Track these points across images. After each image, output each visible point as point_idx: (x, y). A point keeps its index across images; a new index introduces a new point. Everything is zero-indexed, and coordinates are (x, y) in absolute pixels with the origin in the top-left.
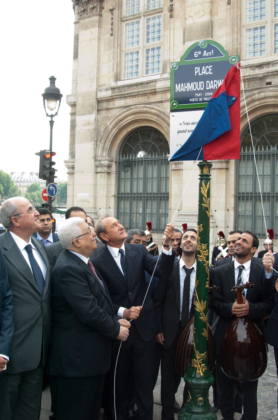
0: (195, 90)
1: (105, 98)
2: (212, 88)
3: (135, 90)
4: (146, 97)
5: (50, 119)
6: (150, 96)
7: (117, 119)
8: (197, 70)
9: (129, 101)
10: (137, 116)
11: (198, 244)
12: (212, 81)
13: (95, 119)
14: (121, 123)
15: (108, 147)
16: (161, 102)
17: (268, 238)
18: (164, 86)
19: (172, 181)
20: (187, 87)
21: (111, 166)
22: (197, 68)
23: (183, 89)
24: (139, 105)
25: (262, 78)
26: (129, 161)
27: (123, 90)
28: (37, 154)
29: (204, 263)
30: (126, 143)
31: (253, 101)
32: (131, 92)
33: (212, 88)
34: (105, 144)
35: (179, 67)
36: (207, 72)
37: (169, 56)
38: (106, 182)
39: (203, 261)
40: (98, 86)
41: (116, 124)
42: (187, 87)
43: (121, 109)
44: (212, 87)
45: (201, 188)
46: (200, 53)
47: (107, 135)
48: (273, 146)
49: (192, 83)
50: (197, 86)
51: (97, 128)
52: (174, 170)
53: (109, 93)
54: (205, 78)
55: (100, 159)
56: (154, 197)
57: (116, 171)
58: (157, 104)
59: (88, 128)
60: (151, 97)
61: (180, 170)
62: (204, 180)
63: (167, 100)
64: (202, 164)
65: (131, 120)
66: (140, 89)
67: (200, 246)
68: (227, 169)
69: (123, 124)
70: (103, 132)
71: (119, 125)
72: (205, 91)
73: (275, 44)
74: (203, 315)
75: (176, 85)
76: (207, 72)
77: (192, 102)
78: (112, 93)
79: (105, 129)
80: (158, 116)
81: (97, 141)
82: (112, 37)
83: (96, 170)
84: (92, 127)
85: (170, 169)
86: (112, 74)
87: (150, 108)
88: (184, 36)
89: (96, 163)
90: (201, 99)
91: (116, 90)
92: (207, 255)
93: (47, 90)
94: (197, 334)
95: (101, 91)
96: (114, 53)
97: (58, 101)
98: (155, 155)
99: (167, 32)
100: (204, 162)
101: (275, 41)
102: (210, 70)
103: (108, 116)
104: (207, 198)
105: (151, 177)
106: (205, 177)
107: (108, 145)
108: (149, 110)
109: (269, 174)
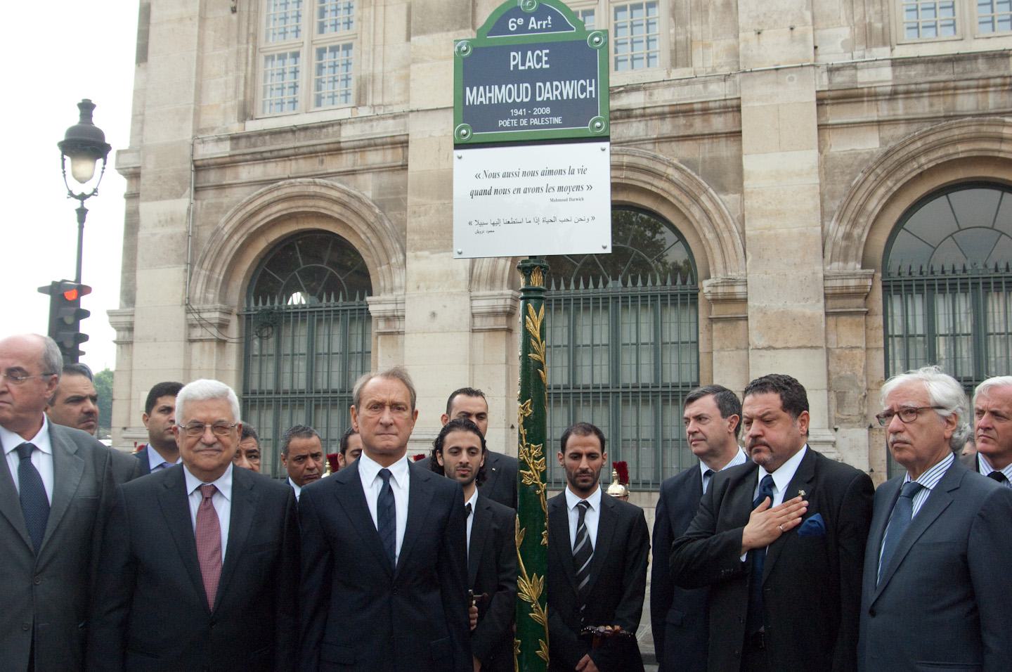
0: (510, 101)
1: (213, 161)
2: (548, 98)
3: (289, 143)
4: (316, 161)
5: (77, 204)
6: (324, 158)
7: (244, 212)
8: (515, 59)
9: (274, 170)
10: (292, 204)
11: (522, 444)
12: (548, 84)
13: (189, 210)
14: (255, 220)
15: (221, 278)
16: (353, 173)
17: (616, 482)
18: (360, 136)
19: (379, 360)
20: (492, 95)
21: (227, 325)
22: (515, 54)
23: (483, 99)
24: (299, 180)
26: (271, 313)
27: (259, 143)
28: (42, 290)
29: (537, 487)
30: (264, 274)
32: (278, 147)
33: (548, 98)
34: (212, 270)
35: (474, 50)
36: (538, 64)
37: (373, 67)
38: (214, 362)
39: (533, 483)
40: (198, 130)
41: (242, 223)
42: (492, 95)
43: (254, 187)
44: (550, 95)
45: (527, 317)
46: (521, 21)
47: (218, 249)
48: (615, 278)
49: (504, 86)
50: (514, 93)
51: (193, 232)
52: (384, 334)
53: (225, 149)
54: (532, 76)
55: (200, 307)
56: (334, 399)
57: (240, 338)
58: (341, 177)
59: (169, 230)
60: (328, 159)
61: (399, 333)
62: (532, 301)
63: (367, 169)
64: (528, 264)
65: (278, 215)
66: (302, 141)
67: (527, 449)
68: (509, 331)
69: (258, 222)
70: (209, 243)
71: (249, 225)
72: (533, 103)
73: (616, 51)
74: (537, 608)
75: (468, 89)
76: (538, 64)
77: (503, 128)
78: (232, 149)
79: (213, 234)
80: (344, 205)
81: (192, 265)
82: (234, 17)
83: (189, 334)
84: (181, 229)
85: (374, 331)
86: (232, 103)
87: (326, 186)
88: (409, 21)
89: (190, 316)
90: (524, 122)
91: (243, 142)
92: (543, 469)
93: (71, 132)
94: (524, 654)
95: (203, 142)
96: (238, 52)
97: (100, 161)
98: (337, 299)
99: (368, 12)
100: (532, 260)
101: (616, 43)
102: (545, 59)
103: (222, 203)
104: (539, 340)
105: (326, 351)
106: (533, 294)
107: (220, 273)
108: (323, 191)
109: (605, 341)
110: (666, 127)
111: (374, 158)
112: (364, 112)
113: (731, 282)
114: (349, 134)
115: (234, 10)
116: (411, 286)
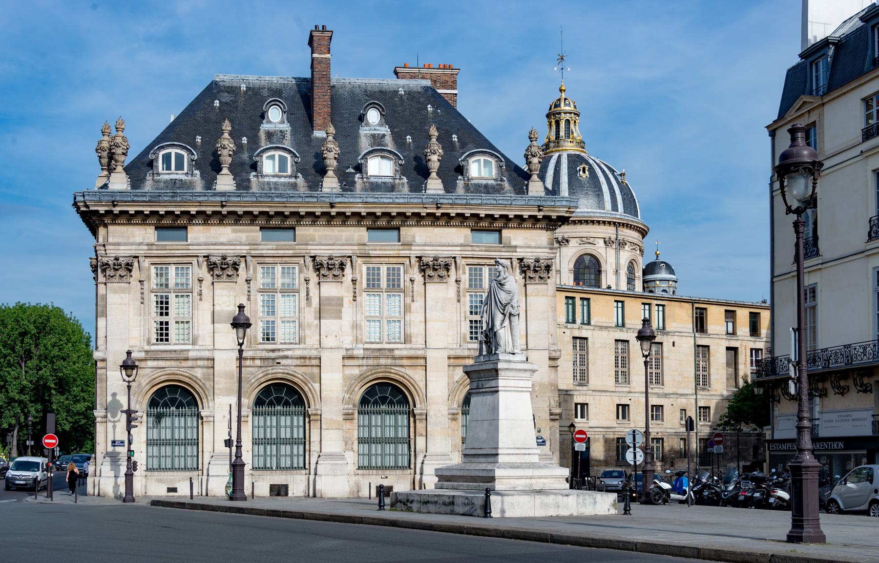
3: (169, 355)
25: (274, 359)
31: (268, 374)
41: (150, 382)
66: (173, 355)
110: (298, 362)
111: (200, 363)
112: (197, 347)
113: (317, 410)
114: (191, 354)
115: (142, 303)
116: (216, 407)
